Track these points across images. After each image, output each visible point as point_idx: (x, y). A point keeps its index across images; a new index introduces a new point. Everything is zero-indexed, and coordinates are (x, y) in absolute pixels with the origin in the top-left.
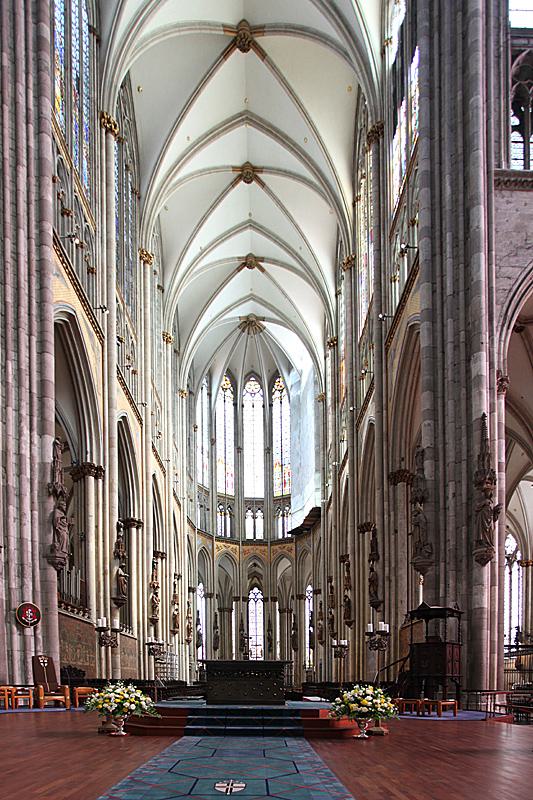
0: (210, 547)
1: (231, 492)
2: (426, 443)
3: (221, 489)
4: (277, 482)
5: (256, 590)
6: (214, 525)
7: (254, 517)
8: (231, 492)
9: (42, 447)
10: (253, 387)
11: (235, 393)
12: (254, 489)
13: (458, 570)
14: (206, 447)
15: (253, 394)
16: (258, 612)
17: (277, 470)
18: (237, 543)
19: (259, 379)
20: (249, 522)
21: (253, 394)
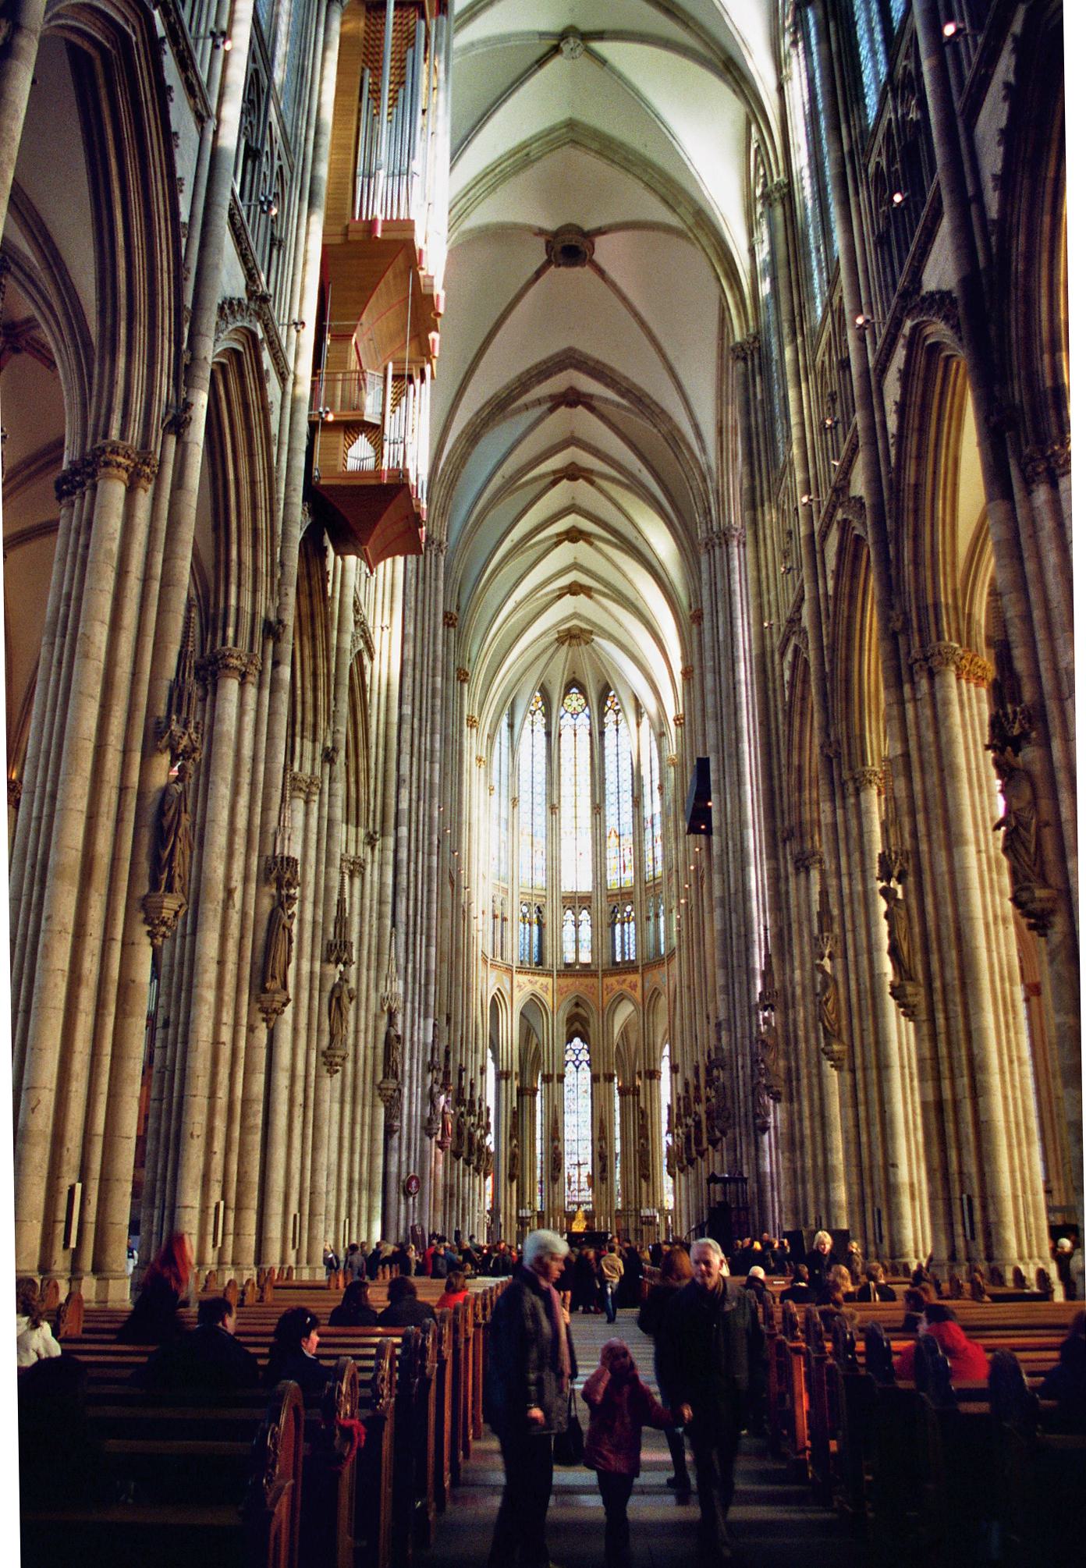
0: (508, 987)
1: (540, 880)
2: (722, 1016)
4: (612, 864)
5: (577, 1041)
7: (577, 925)
9: (425, 1029)
10: (575, 704)
11: (547, 715)
13: (748, 1135)
15: (575, 715)
16: (581, 1089)
17: (612, 842)
18: (549, 974)
19: (583, 691)
20: (569, 930)
21: (575, 715)
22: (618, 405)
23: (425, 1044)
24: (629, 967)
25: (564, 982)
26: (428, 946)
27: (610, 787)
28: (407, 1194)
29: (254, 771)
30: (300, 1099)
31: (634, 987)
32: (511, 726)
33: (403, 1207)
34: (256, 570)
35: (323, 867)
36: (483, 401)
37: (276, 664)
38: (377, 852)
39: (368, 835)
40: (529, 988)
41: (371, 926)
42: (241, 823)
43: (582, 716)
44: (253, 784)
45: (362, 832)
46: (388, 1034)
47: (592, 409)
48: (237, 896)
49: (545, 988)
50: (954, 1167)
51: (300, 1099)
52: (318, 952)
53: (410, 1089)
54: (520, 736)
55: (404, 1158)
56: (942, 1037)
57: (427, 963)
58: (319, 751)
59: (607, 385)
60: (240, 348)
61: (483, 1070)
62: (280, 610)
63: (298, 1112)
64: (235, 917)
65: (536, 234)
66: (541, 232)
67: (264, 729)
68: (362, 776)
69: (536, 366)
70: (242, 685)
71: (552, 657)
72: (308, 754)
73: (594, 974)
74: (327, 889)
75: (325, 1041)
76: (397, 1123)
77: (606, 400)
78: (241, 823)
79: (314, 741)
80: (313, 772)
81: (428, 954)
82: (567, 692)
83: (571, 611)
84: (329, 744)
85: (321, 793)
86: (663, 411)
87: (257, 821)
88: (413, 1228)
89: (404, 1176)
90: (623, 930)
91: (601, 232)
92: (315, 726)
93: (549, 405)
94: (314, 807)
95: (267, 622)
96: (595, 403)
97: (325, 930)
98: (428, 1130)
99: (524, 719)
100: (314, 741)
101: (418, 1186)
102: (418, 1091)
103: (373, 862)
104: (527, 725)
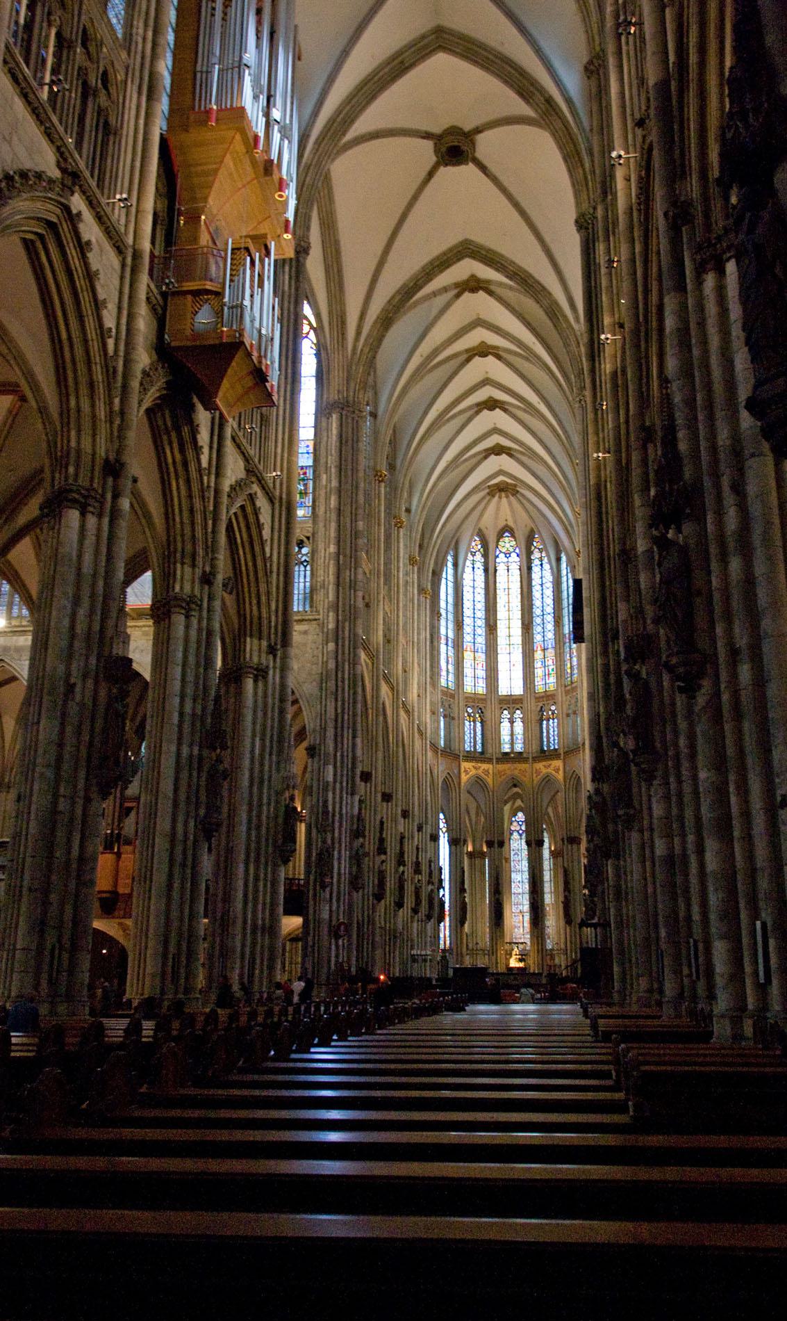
1: (481, 688)
3: (469, 687)
4: (539, 672)
5: (520, 815)
6: (462, 740)
7: (512, 722)
8: (481, 688)
10: (508, 545)
11: (485, 555)
12: (511, 682)
14: (451, 635)
15: (508, 555)
17: (538, 655)
19: (513, 536)
20: (505, 727)
21: (508, 555)
22: (511, 288)
23: (352, 817)
24: (554, 755)
25: (501, 767)
26: (354, 737)
27: (537, 611)
28: (337, 937)
29: (93, 585)
30: (179, 858)
31: (557, 770)
32: (455, 565)
33: (333, 947)
34: (94, 416)
35: (202, 670)
36: (393, 291)
37: (116, 496)
38: (278, 660)
39: (270, 646)
40: (473, 772)
41: (273, 719)
42: (80, 628)
43: (514, 555)
44: (93, 596)
45: (264, 643)
46: (287, 806)
47: (490, 293)
48: (78, 689)
49: (486, 772)
50: (682, 914)
51: (179, 858)
52: (197, 738)
53: (339, 852)
54: (463, 571)
55: (334, 908)
56: (674, 799)
57: (353, 751)
58: (198, 572)
59: (497, 270)
60: (55, 220)
61: (435, 838)
62: (119, 452)
63: (177, 870)
64: (73, 709)
65: (423, 138)
66: (427, 136)
67: (104, 550)
68: (263, 598)
69: (438, 258)
70: (83, 514)
71: (485, 508)
72: (188, 576)
73: (525, 760)
74: (206, 689)
75: (202, 812)
76: (328, 880)
77: (501, 284)
78: (80, 628)
79: (194, 566)
80: (193, 588)
81: (354, 745)
82: (500, 536)
83: (497, 469)
84: (208, 569)
85: (201, 610)
86: (544, 289)
87: (96, 627)
88: (341, 964)
89: (334, 923)
90: (548, 725)
91: (478, 131)
92: (194, 556)
93: (455, 292)
94: (195, 621)
95: (107, 461)
96: (492, 288)
97: (203, 722)
98: (355, 883)
99: (466, 559)
100: (194, 566)
101: (346, 930)
102: (345, 854)
103: (274, 668)
104: (468, 563)
